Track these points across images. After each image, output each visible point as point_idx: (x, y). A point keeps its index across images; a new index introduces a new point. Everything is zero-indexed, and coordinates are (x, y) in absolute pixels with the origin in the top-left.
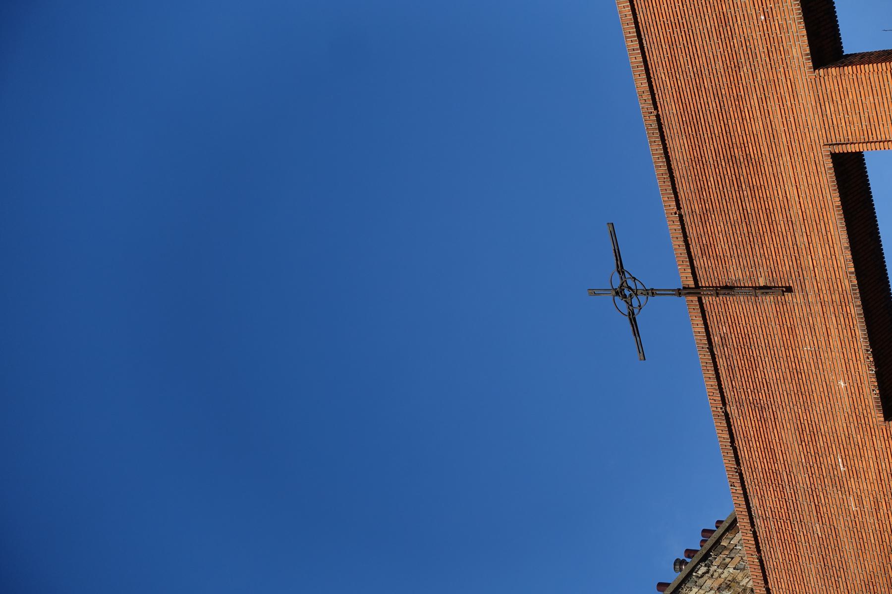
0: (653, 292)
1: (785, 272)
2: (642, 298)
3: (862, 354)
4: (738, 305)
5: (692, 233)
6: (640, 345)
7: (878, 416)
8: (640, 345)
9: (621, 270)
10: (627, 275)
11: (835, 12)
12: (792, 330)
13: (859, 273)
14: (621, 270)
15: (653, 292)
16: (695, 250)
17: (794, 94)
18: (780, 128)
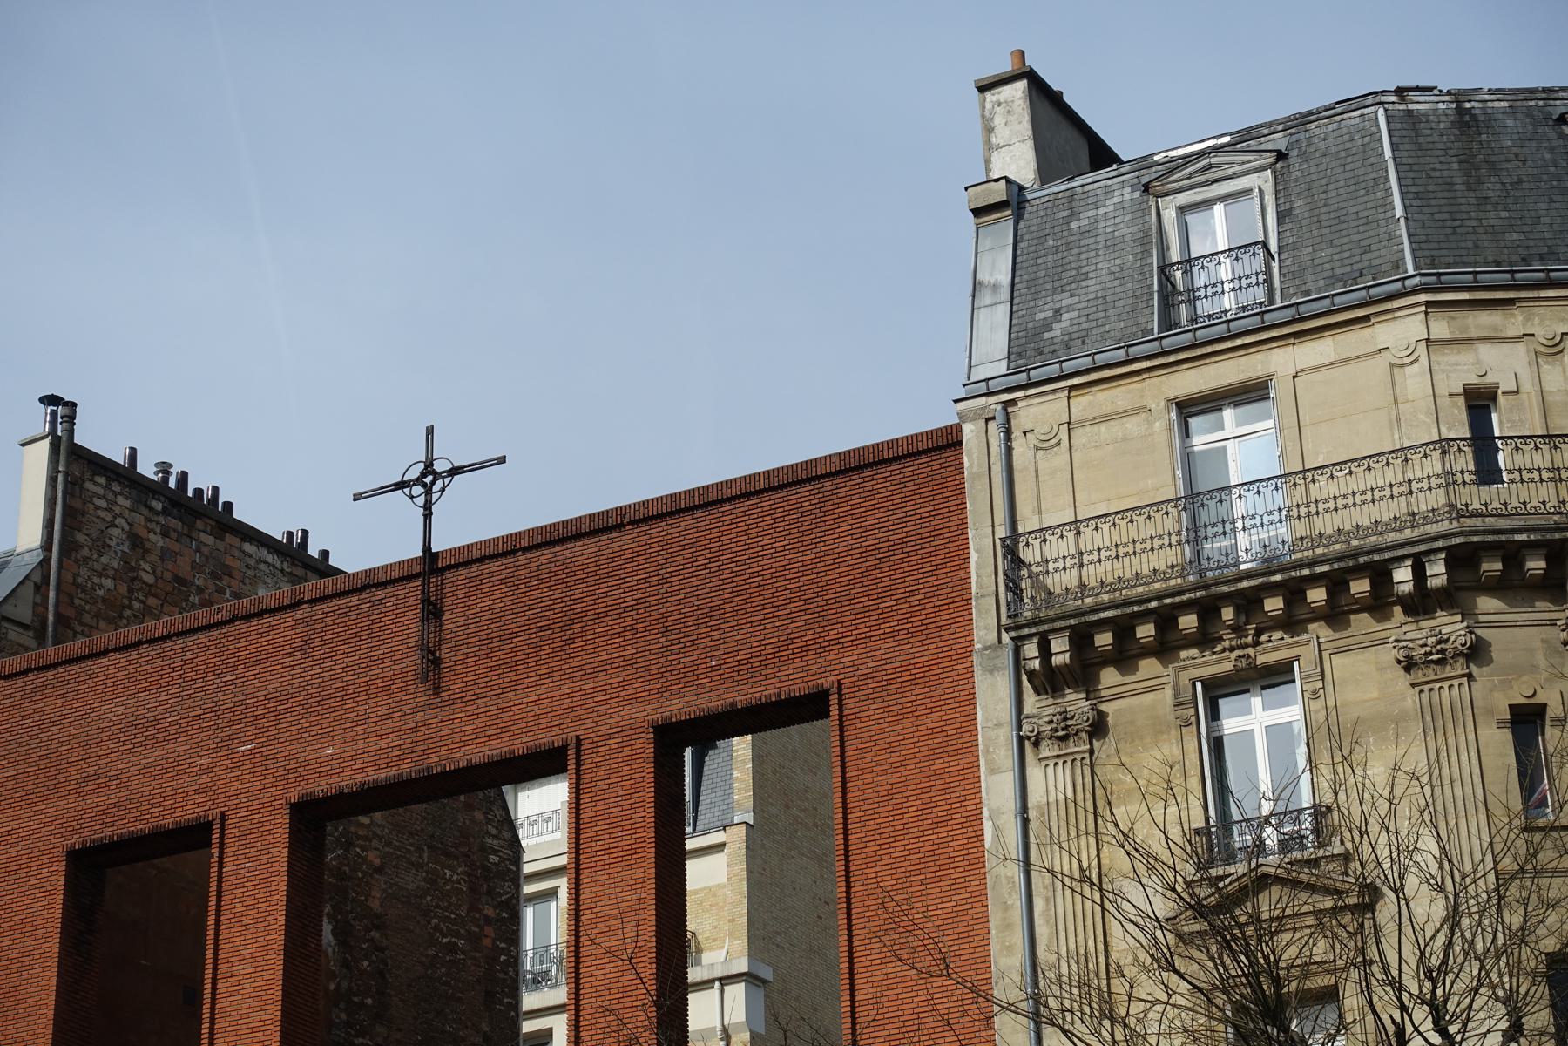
0: (428, 516)
1: (453, 685)
2: (421, 501)
3: (361, 778)
4: (411, 626)
5: (496, 565)
6: (371, 494)
7: (294, 795)
8: (371, 494)
9: (455, 471)
10: (447, 480)
11: (715, 747)
12: (388, 690)
13: (444, 775)
14: (455, 471)
15: (428, 516)
16: (475, 570)
17: (634, 700)
18: (602, 680)
